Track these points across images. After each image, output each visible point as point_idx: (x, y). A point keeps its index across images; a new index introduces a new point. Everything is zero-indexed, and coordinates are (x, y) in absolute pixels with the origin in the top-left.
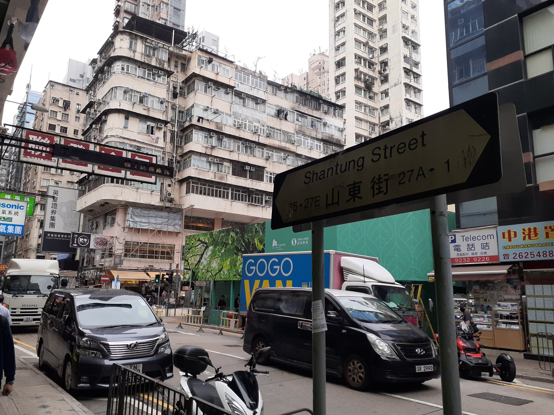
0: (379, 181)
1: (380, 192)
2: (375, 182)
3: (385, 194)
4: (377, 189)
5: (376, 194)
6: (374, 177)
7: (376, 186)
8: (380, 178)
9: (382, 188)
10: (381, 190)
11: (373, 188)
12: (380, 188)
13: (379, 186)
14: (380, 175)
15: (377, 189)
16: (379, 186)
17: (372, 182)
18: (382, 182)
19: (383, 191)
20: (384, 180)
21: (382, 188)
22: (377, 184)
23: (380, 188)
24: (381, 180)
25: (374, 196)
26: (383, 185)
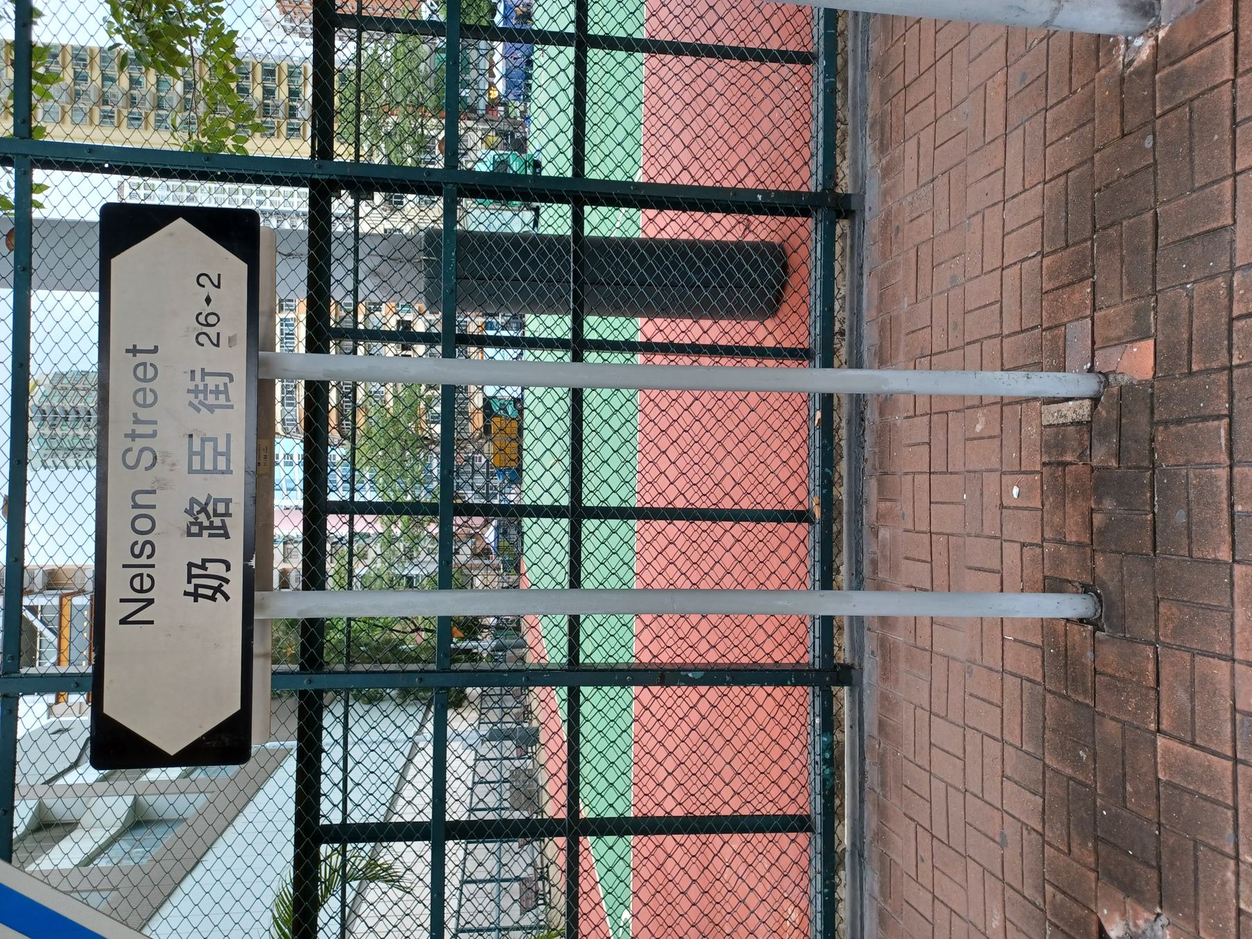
0: (201, 392)
1: (226, 392)
2: (200, 402)
3: (231, 380)
4: (217, 399)
5: (228, 399)
6: (191, 404)
7: (211, 399)
8: (195, 391)
9: (217, 386)
10: (222, 388)
11: (211, 408)
12: (217, 392)
13: (211, 392)
14: (189, 391)
15: (217, 399)
16: (211, 392)
17: (198, 410)
18: (206, 386)
19: (225, 384)
20: (203, 380)
21: (217, 386)
22: (206, 398)
23: (217, 392)
24: (201, 387)
25: (232, 407)
26: (211, 382)
